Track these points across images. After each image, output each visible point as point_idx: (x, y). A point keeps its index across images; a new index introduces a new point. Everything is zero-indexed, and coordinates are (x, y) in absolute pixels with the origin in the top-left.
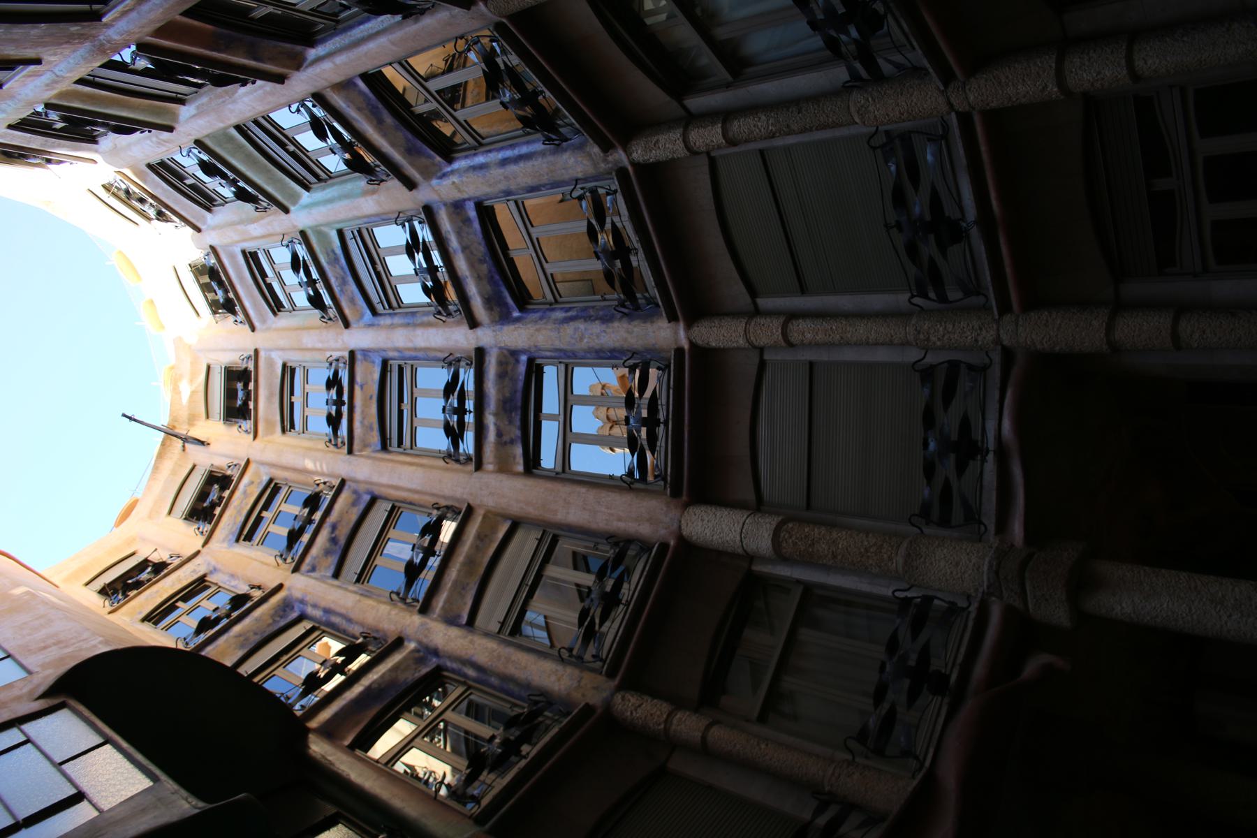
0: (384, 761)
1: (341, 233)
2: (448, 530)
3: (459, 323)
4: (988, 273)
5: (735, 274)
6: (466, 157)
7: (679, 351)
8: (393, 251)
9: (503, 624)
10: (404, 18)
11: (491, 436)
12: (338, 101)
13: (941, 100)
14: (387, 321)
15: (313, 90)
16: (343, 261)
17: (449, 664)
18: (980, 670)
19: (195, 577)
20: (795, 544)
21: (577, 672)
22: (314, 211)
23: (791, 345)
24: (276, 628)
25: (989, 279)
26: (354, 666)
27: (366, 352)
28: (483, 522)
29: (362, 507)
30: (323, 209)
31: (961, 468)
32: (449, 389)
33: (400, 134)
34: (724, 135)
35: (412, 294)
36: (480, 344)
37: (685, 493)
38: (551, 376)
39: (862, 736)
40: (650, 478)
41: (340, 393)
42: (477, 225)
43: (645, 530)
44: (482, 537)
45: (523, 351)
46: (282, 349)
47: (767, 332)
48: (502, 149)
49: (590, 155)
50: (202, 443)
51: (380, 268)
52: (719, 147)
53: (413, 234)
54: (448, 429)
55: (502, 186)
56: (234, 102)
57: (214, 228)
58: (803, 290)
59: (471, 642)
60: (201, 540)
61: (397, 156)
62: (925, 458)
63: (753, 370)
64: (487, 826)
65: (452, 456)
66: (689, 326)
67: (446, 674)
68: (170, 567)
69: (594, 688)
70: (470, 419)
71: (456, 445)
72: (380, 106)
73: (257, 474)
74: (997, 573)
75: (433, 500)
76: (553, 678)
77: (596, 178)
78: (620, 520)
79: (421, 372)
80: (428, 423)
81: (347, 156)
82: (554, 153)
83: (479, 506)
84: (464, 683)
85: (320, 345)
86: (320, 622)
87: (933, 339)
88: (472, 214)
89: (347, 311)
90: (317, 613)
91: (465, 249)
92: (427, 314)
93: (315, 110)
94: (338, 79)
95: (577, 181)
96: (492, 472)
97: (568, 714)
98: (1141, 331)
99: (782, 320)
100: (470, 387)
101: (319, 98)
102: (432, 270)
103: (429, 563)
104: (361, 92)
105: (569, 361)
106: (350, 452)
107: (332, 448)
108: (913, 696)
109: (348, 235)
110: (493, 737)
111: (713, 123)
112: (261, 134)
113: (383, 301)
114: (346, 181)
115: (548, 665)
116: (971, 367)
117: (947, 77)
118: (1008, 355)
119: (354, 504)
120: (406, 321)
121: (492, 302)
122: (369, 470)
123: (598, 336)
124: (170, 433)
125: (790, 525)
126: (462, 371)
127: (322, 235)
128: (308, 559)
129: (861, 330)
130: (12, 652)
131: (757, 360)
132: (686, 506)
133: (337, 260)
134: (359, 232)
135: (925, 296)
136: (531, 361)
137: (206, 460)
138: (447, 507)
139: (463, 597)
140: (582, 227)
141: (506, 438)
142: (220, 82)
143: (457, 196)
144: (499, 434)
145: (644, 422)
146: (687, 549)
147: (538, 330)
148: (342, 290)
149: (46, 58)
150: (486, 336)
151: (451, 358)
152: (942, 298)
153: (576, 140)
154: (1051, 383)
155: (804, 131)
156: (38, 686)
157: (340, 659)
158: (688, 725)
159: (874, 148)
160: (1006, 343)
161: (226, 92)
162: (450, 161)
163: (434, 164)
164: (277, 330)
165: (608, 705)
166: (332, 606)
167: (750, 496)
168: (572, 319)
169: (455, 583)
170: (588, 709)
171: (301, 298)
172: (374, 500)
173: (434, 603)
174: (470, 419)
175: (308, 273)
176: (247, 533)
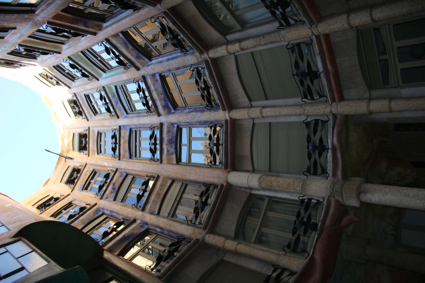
0: (129, 259)
1: (116, 87)
2: (151, 183)
3: (154, 115)
4: (327, 89)
5: (244, 94)
6: (156, 59)
7: (226, 121)
8: (133, 92)
9: (169, 214)
10: (134, 11)
11: (165, 152)
12: (114, 41)
14: (131, 115)
15: (105, 38)
17: (151, 227)
18: (328, 222)
19: (68, 202)
21: (193, 228)
22: (107, 80)
24: (94, 217)
25: (327, 91)
26: (119, 229)
27: (124, 126)
28: (162, 180)
30: (110, 79)
31: (320, 155)
32: (151, 137)
33: (134, 52)
35: (139, 106)
36: (162, 122)
37: (229, 168)
38: (185, 132)
39: (289, 246)
40: (217, 164)
41: (116, 140)
43: (215, 181)
44: (162, 185)
46: (97, 127)
47: (255, 113)
48: (167, 56)
49: (196, 56)
50: (71, 159)
51: (129, 98)
52: (238, 51)
53: (139, 86)
54: (151, 150)
55: (168, 68)
56: (80, 43)
57: (75, 87)
58: (267, 99)
59: (159, 220)
60: (71, 190)
61: (133, 59)
62: (308, 152)
63: (251, 126)
64: (162, 279)
65: (152, 159)
66: (229, 112)
67: (150, 231)
68: (60, 199)
69: (199, 233)
70: (158, 147)
71: (154, 155)
72: (127, 42)
73: (89, 168)
74: (333, 189)
75: (146, 174)
76: (185, 230)
77: (198, 64)
78: (207, 177)
79: (142, 132)
80: (145, 149)
81: (117, 60)
82: (184, 56)
83: (161, 175)
84: (156, 234)
85: (109, 125)
86: (109, 215)
87: (310, 112)
88: (158, 78)
89: (118, 113)
90: (108, 212)
91: (156, 90)
92: (144, 113)
93: (106, 45)
94: (113, 33)
95: (192, 65)
96: (166, 164)
97: (190, 242)
98: (377, 106)
100: (158, 136)
101: (108, 40)
102: (145, 97)
103: (145, 195)
104: (121, 38)
105: (190, 126)
106: (119, 159)
107: (113, 158)
108: (305, 232)
109: (118, 88)
110: (165, 250)
111: (236, 43)
112: (89, 54)
113: (130, 109)
114: (117, 69)
115: (184, 226)
118: (335, 116)
119: (121, 176)
120: (137, 115)
121: (165, 107)
122: (126, 165)
123: (200, 117)
124: (61, 156)
125: (264, 177)
126: (155, 131)
127: (110, 88)
128: (105, 195)
129: (285, 111)
130: (4, 224)
131: (252, 123)
133: (115, 96)
134: (122, 86)
135: (306, 98)
136: (178, 127)
137: (73, 164)
138: (151, 176)
139: (156, 205)
140: (194, 80)
141: (170, 152)
142: (75, 35)
143: (153, 72)
144: (168, 151)
145: (215, 145)
147: (180, 116)
148: (116, 106)
149: (18, 27)
150: (163, 119)
151: (152, 127)
152: (312, 99)
153: (191, 51)
155: (265, 44)
156: (12, 234)
157: (115, 227)
158: (230, 245)
159: (288, 49)
161: (77, 40)
162: (150, 60)
163: (145, 62)
164: (95, 120)
165: (203, 239)
166: (113, 210)
167: (251, 168)
169: (153, 201)
170: (197, 240)
171: (103, 110)
172: (127, 175)
173: (146, 207)
174: (158, 147)
175: (105, 101)
176: (86, 188)
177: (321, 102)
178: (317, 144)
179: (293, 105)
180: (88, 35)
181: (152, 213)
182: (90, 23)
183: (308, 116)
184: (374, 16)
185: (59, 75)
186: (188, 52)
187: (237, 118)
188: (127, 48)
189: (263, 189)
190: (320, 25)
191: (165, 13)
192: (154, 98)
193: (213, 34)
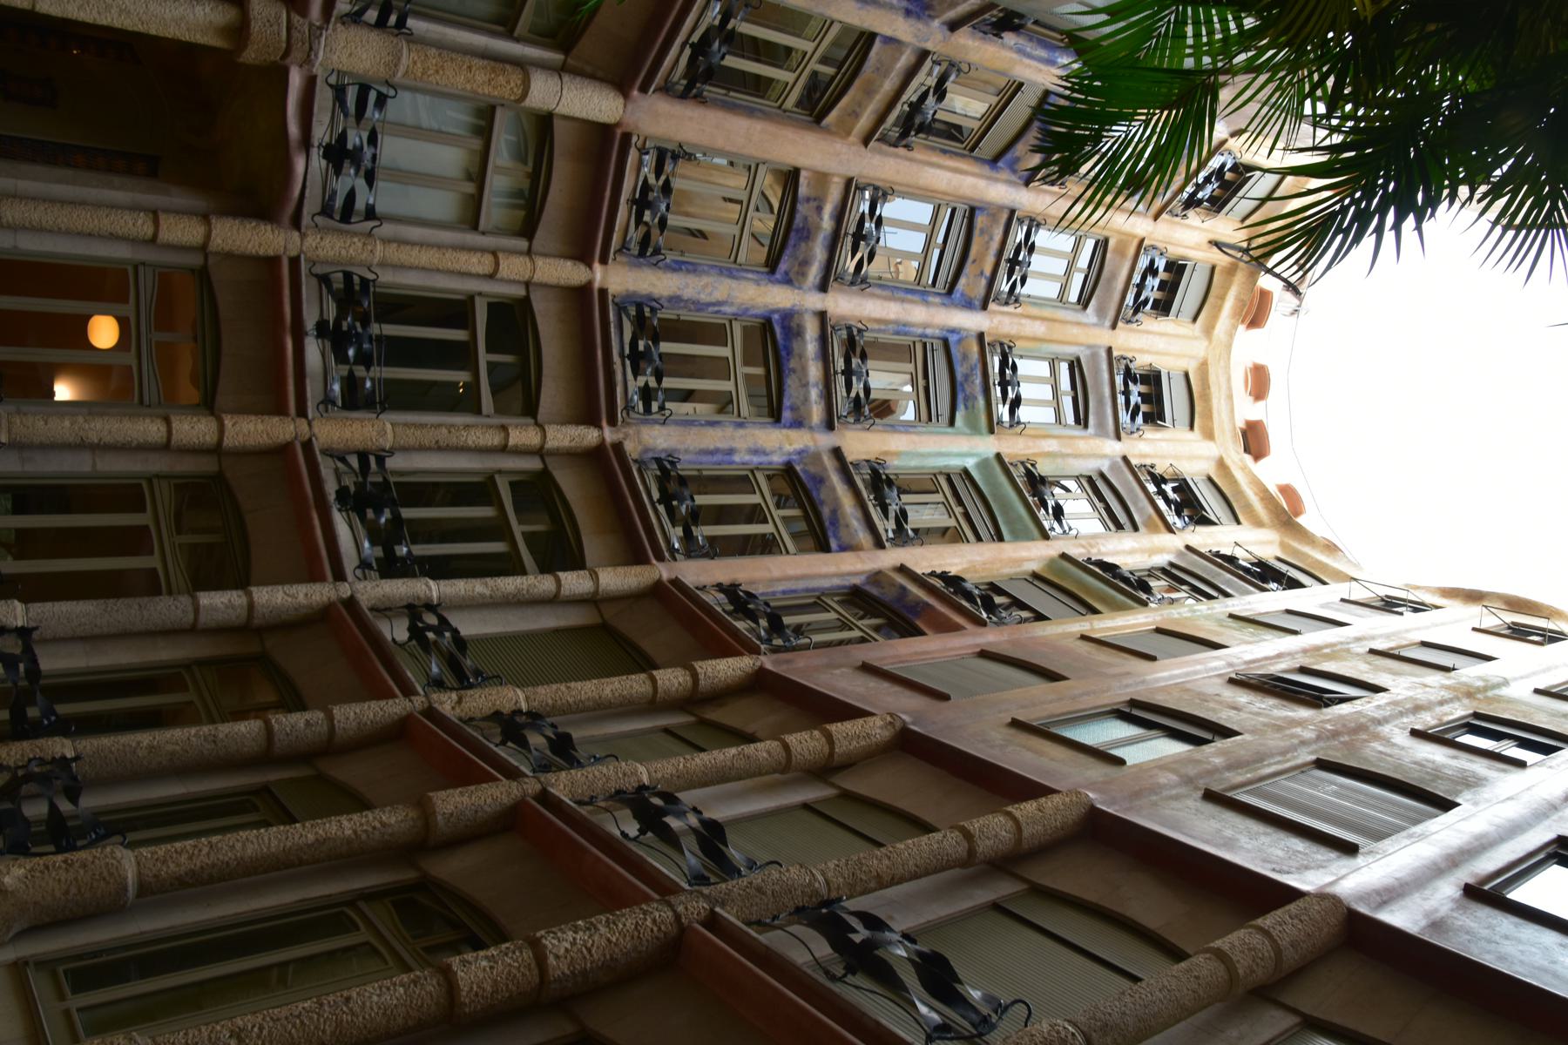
1: (952, 423)
3: (843, 318)
11: (828, 210)
12: (864, 537)
13: (316, 430)
14: (929, 331)
16: (960, 397)
20: (508, 82)
23: (494, 253)
27: (968, 305)
29: (1009, 156)
34: (508, 435)
37: (618, 136)
42: (787, 403)
44: (856, 115)
45: (779, 282)
46: (1078, 324)
47: (514, 267)
51: (921, 382)
55: (741, 432)
57: (1105, 456)
61: (835, 479)
63: (540, 234)
66: (590, 284)
72: (827, 523)
75: (916, 154)
77: (645, 422)
78: (691, 119)
85: (1023, 321)
88: (787, 415)
89: (975, 348)
91: (805, 385)
98: (182, 231)
99: (499, 276)
104: (835, 536)
106: (1013, 212)
107: (1039, 218)
116: (331, 217)
117: (308, 446)
118: (296, 223)
119: (1017, 160)
132: (618, 125)
133: (966, 399)
134: (930, 419)
138: (895, 146)
141: (813, 204)
143: (794, 434)
144: (819, 209)
146: (622, 85)
150: (814, 301)
152: (348, 276)
154: (262, 198)
155: (440, 425)
160: (296, 234)
166: (1042, 67)
168: (714, 304)
169: (886, 75)
173: (913, 59)
177: (326, 262)
178: (347, 164)
179: (402, 267)
180: (919, 572)
181: (889, 40)
182: (888, 595)
183: (370, 234)
184: (163, 429)
185: (1135, 504)
186: (663, 456)
187: (569, 263)
188: (834, 512)
189: (521, 65)
190: (288, 437)
191: (660, 558)
192: (820, 365)
193: (569, 482)
